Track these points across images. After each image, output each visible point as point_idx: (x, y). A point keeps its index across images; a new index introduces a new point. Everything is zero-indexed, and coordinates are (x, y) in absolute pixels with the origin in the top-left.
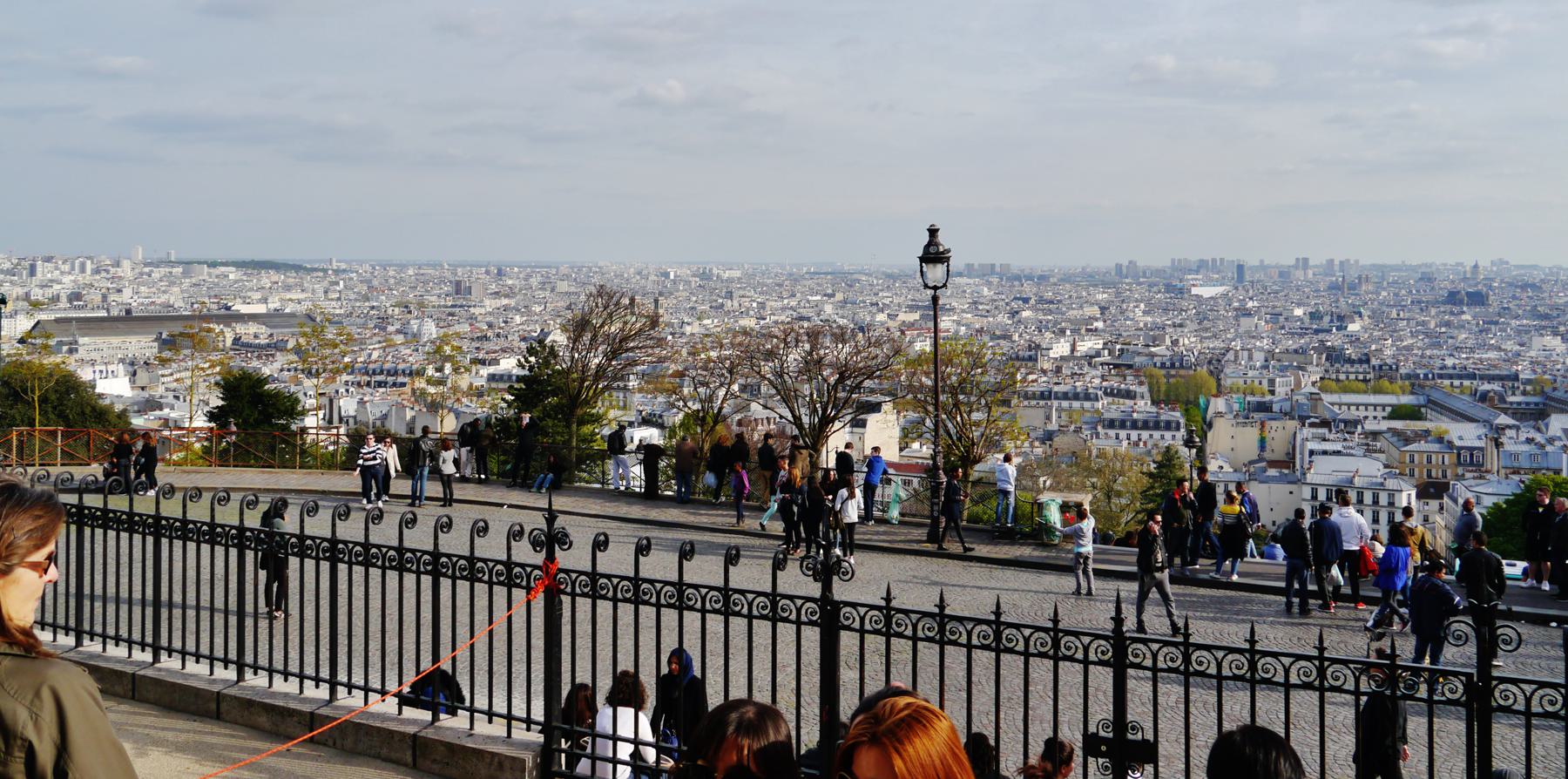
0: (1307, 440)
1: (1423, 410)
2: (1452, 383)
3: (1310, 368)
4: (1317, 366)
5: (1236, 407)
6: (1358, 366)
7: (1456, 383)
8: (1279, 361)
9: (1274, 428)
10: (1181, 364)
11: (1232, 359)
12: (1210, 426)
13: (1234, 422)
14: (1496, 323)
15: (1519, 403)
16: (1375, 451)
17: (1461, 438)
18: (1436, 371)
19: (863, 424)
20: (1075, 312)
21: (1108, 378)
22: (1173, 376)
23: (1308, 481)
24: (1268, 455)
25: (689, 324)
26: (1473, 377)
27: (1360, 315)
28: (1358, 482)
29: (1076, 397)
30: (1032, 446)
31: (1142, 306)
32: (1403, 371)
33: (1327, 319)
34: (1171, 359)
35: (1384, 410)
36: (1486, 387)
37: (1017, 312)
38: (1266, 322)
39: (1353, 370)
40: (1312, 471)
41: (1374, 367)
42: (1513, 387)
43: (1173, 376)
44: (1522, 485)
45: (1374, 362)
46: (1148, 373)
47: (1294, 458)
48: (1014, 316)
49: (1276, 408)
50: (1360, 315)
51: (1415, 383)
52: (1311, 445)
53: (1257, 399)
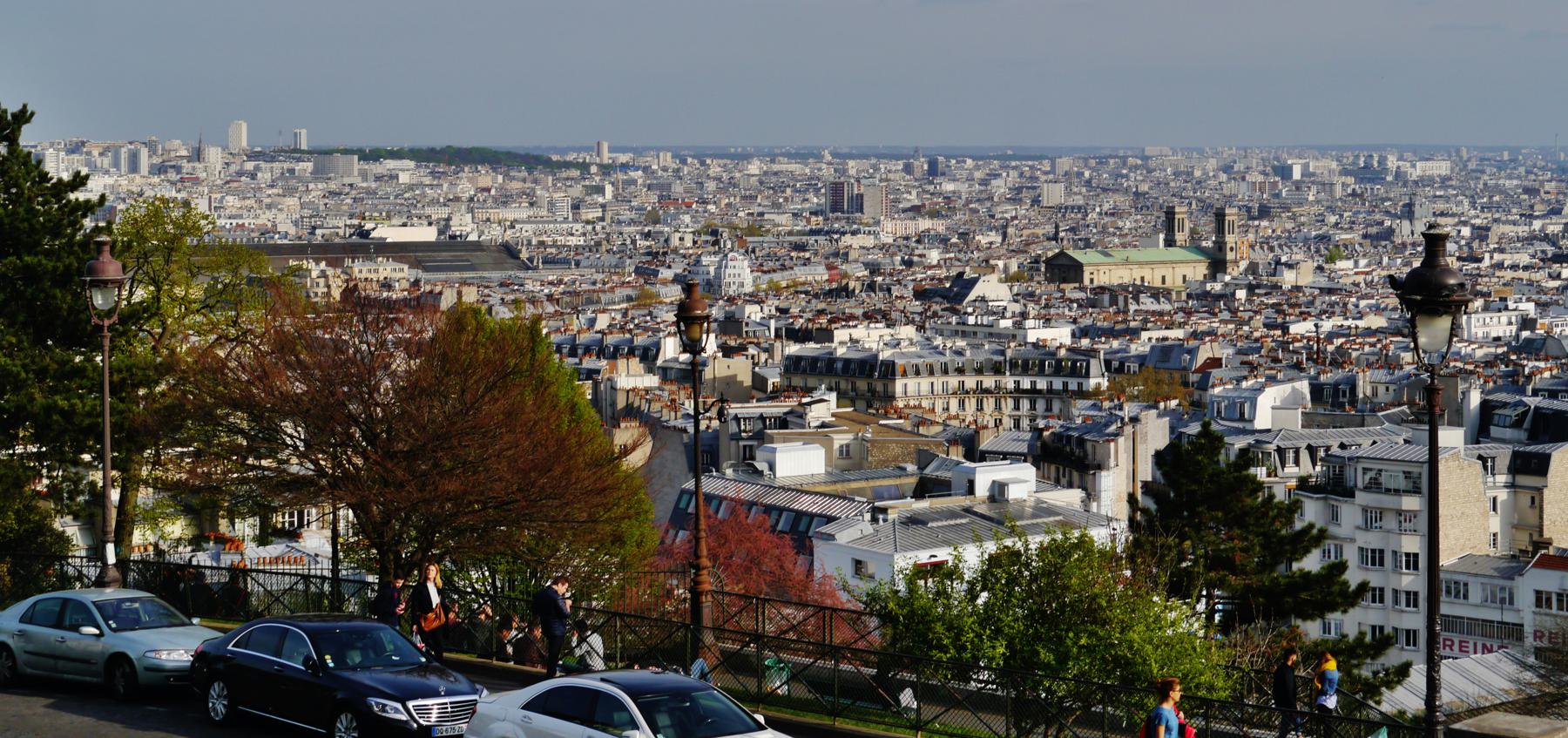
19: (1539, 466)
25: (1290, 266)
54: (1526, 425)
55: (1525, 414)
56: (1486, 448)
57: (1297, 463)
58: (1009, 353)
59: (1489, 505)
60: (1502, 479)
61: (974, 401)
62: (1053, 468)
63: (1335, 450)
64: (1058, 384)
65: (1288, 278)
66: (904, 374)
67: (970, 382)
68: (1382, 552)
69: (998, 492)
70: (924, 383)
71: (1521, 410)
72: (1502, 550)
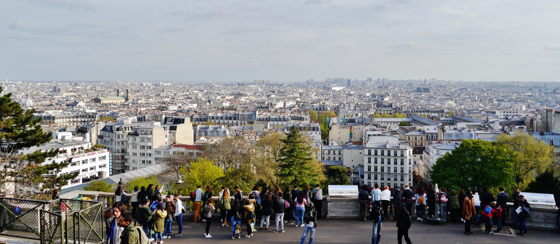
1: (411, 123)
2: (421, 114)
3: (371, 110)
4: (373, 109)
5: (341, 121)
6: (388, 108)
7: (422, 114)
8: (360, 107)
9: (355, 129)
10: (324, 109)
11: (343, 107)
12: (330, 129)
13: (340, 127)
14: (433, 97)
15: (444, 120)
16: (395, 134)
17: (428, 129)
18: (415, 110)
20: (291, 95)
21: (294, 113)
22: (321, 113)
23: (367, 147)
24: (353, 140)
25: (140, 100)
26: (428, 111)
27: (389, 95)
28: (388, 146)
29: (280, 120)
30: (256, 138)
31: (314, 93)
32: (404, 110)
33: (377, 97)
34: (320, 107)
35: (397, 124)
36: (433, 115)
37: (269, 96)
38: (357, 98)
39: (386, 110)
40: (369, 142)
41: (393, 108)
43: (321, 113)
44: (456, 145)
45: (393, 107)
46: (311, 112)
47: (363, 141)
48: (268, 97)
49: (356, 121)
50: (389, 95)
51: (408, 114)
52: (369, 133)
54: (173, 121)
55: (173, 119)
56: (165, 126)
57: (128, 130)
58: (79, 114)
60: (168, 131)
61: (72, 123)
62: (80, 134)
63: (136, 127)
64: (89, 119)
65: (140, 102)
66: (57, 119)
67: (71, 120)
68: (144, 146)
69: (63, 138)
70: (62, 120)
71: (172, 118)
72: (168, 144)
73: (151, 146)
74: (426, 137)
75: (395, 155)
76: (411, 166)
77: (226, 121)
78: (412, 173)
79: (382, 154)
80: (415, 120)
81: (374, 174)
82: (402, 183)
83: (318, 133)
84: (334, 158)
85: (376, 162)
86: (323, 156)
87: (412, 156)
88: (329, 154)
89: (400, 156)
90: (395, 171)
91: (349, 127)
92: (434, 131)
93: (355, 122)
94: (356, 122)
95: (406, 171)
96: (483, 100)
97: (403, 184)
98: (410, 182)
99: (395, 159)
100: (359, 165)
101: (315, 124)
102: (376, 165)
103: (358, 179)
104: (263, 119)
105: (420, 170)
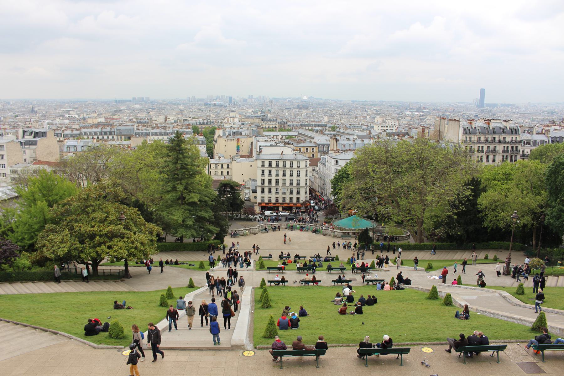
0: (258, 141)
11: (227, 121)
12: (216, 142)
14: (312, 114)
21: (176, 127)
24: (241, 153)
29: (161, 134)
37: (149, 113)
41: (278, 122)
42: (325, 129)
47: (252, 153)
49: (243, 133)
53: (236, 130)
54: (33, 135)
59: (23, 152)
73: (4, 165)
74: (317, 148)
75: (290, 166)
76: (308, 178)
77: (100, 137)
78: (308, 186)
79: (277, 165)
80: (301, 134)
81: (268, 188)
82: (298, 196)
83: (203, 146)
84: (222, 172)
85: (270, 174)
86: (210, 170)
87: (308, 168)
88: (217, 167)
89: (296, 167)
90: (290, 184)
91: (236, 140)
92: (326, 143)
93: (241, 134)
94: (243, 134)
95: (302, 184)
96: (358, 117)
97: (299, 198)
98: (306, 196)
99: (290, 171)
100: (250, 179)
101: (199, 137)
102: (270, 178)
103: (248, 194)
104: (142, 133)
105: (314, 183)
